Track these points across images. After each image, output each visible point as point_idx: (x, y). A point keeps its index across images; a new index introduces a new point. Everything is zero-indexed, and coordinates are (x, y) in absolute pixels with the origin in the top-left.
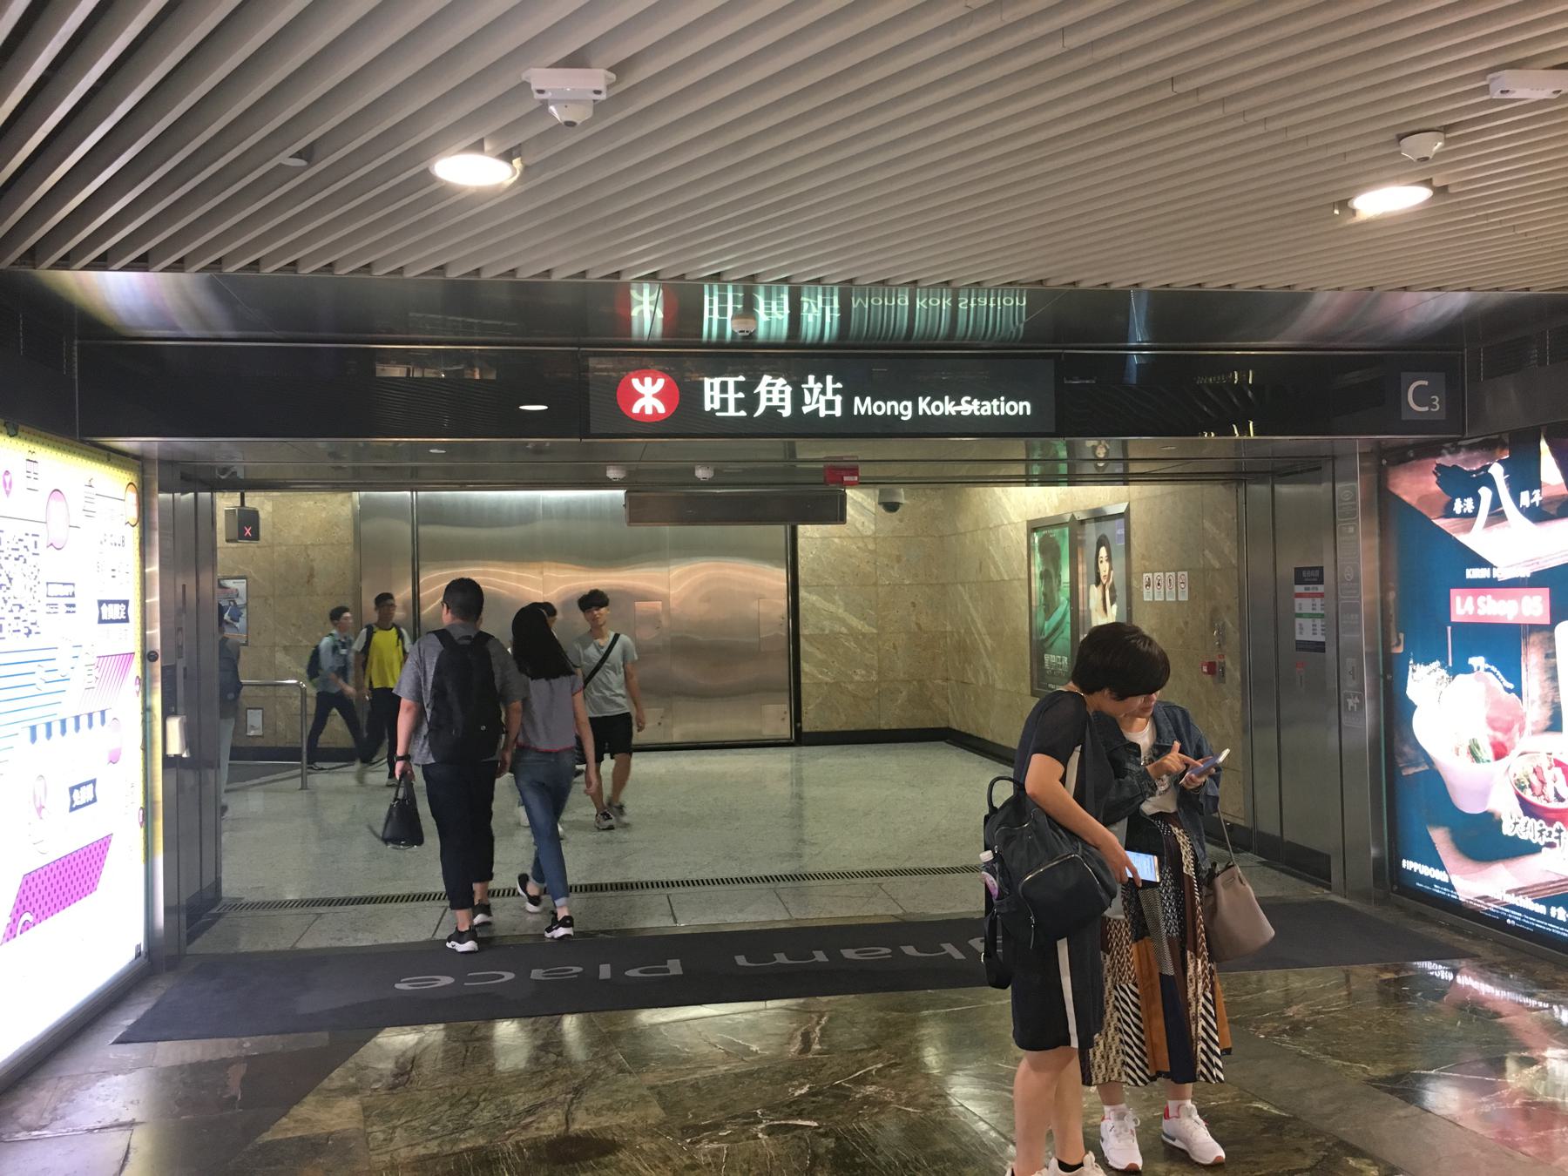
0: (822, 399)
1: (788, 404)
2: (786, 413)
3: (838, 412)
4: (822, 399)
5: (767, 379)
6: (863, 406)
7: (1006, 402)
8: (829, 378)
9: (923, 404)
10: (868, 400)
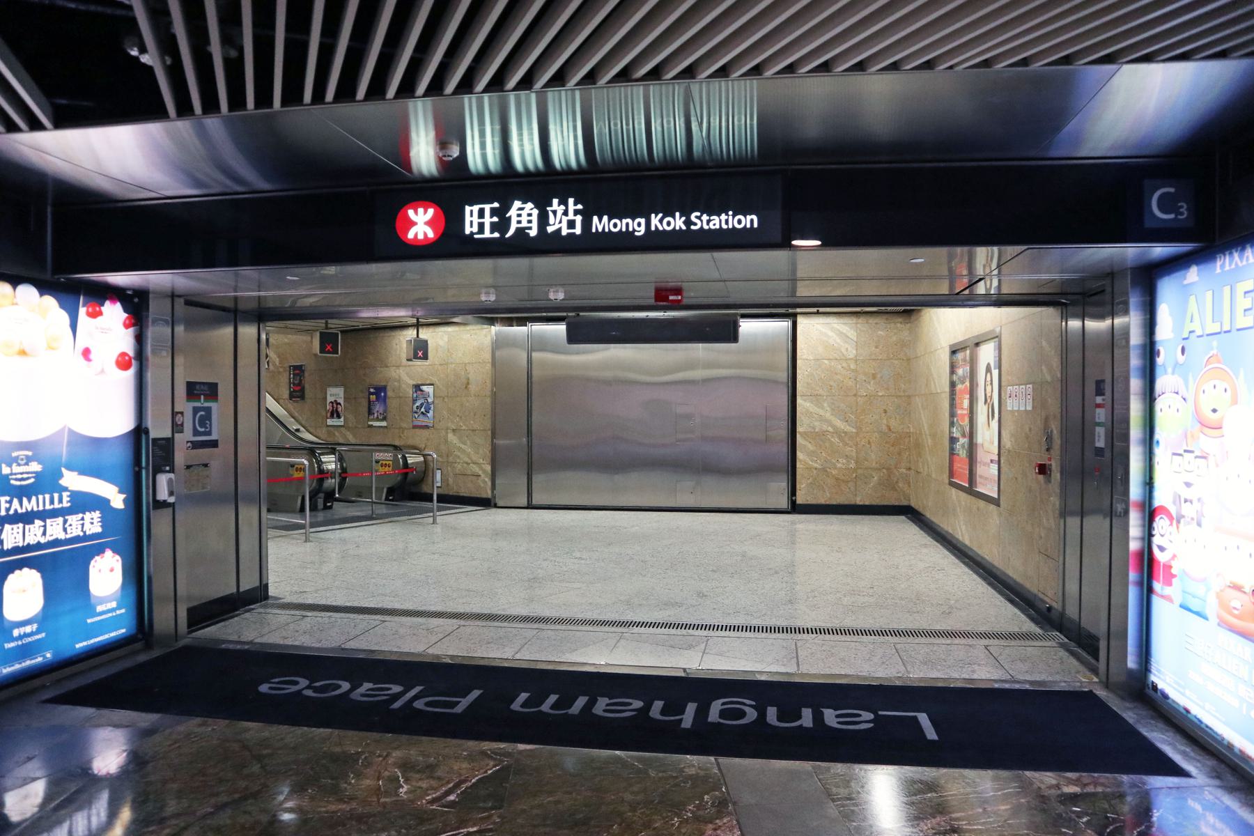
0: (565, 219)
1: (535, 225)
2: (533, 233)
3: (578, 231)
4: (565, 219)
5: (517, 204)
6: (600, 224)
7: (734, 216)
8: (571, 201)
10: (605, 218)
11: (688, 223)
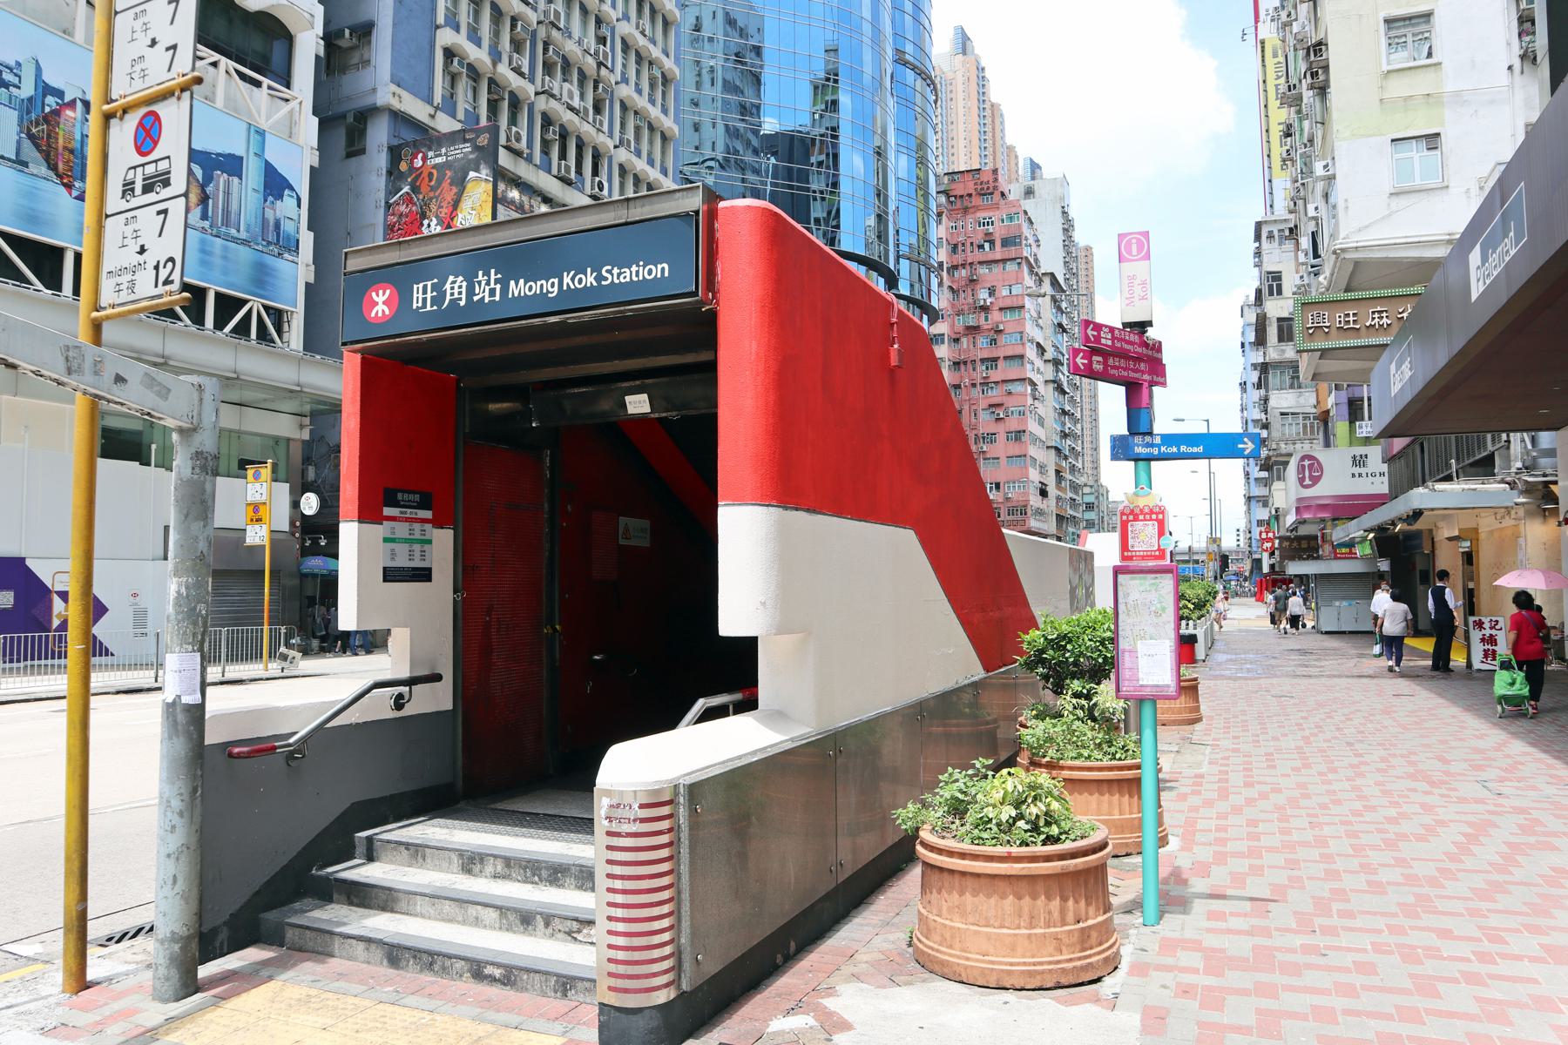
1: (464, 296)
2: (462, 303)
3: (497, 298)
9: (567, 280)
10: (522, 281)
11: (600, 278)
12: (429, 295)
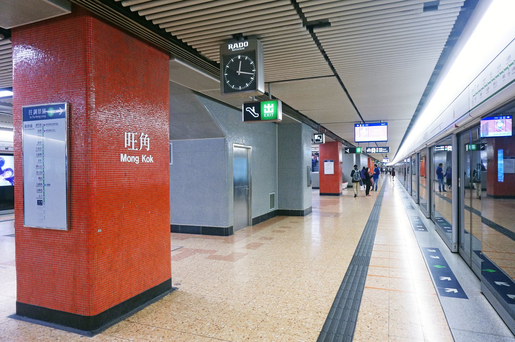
1: (148, 145)
12: (133, 141)
